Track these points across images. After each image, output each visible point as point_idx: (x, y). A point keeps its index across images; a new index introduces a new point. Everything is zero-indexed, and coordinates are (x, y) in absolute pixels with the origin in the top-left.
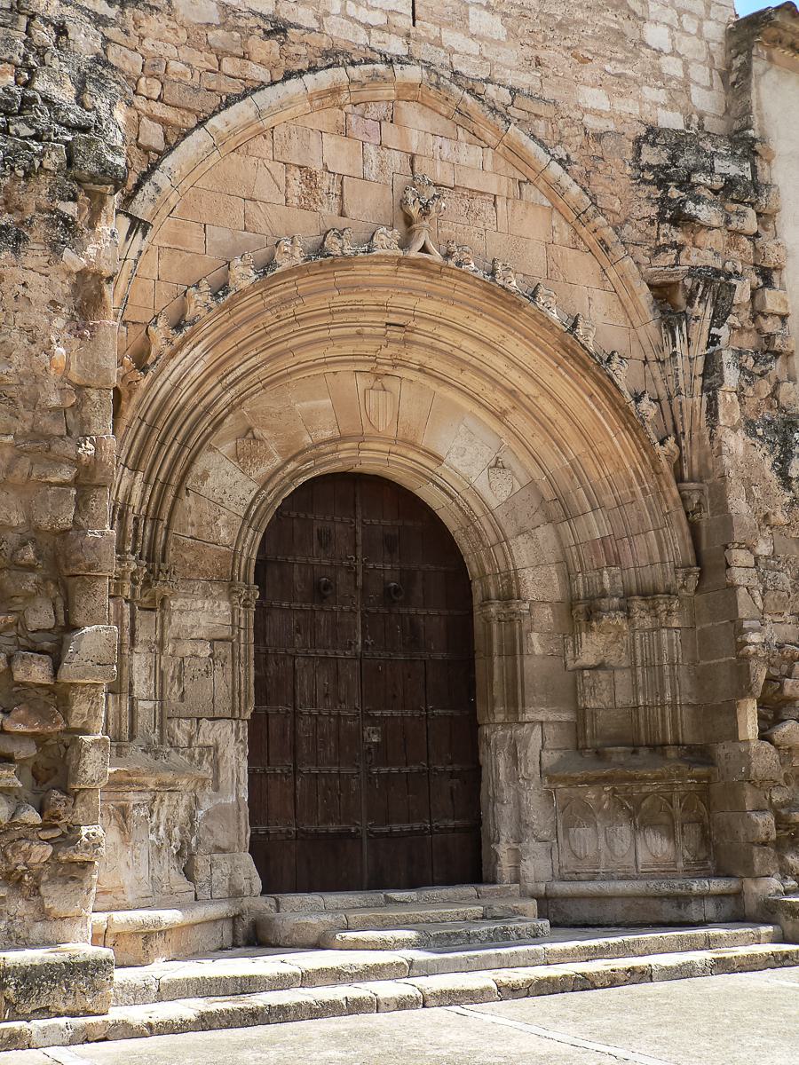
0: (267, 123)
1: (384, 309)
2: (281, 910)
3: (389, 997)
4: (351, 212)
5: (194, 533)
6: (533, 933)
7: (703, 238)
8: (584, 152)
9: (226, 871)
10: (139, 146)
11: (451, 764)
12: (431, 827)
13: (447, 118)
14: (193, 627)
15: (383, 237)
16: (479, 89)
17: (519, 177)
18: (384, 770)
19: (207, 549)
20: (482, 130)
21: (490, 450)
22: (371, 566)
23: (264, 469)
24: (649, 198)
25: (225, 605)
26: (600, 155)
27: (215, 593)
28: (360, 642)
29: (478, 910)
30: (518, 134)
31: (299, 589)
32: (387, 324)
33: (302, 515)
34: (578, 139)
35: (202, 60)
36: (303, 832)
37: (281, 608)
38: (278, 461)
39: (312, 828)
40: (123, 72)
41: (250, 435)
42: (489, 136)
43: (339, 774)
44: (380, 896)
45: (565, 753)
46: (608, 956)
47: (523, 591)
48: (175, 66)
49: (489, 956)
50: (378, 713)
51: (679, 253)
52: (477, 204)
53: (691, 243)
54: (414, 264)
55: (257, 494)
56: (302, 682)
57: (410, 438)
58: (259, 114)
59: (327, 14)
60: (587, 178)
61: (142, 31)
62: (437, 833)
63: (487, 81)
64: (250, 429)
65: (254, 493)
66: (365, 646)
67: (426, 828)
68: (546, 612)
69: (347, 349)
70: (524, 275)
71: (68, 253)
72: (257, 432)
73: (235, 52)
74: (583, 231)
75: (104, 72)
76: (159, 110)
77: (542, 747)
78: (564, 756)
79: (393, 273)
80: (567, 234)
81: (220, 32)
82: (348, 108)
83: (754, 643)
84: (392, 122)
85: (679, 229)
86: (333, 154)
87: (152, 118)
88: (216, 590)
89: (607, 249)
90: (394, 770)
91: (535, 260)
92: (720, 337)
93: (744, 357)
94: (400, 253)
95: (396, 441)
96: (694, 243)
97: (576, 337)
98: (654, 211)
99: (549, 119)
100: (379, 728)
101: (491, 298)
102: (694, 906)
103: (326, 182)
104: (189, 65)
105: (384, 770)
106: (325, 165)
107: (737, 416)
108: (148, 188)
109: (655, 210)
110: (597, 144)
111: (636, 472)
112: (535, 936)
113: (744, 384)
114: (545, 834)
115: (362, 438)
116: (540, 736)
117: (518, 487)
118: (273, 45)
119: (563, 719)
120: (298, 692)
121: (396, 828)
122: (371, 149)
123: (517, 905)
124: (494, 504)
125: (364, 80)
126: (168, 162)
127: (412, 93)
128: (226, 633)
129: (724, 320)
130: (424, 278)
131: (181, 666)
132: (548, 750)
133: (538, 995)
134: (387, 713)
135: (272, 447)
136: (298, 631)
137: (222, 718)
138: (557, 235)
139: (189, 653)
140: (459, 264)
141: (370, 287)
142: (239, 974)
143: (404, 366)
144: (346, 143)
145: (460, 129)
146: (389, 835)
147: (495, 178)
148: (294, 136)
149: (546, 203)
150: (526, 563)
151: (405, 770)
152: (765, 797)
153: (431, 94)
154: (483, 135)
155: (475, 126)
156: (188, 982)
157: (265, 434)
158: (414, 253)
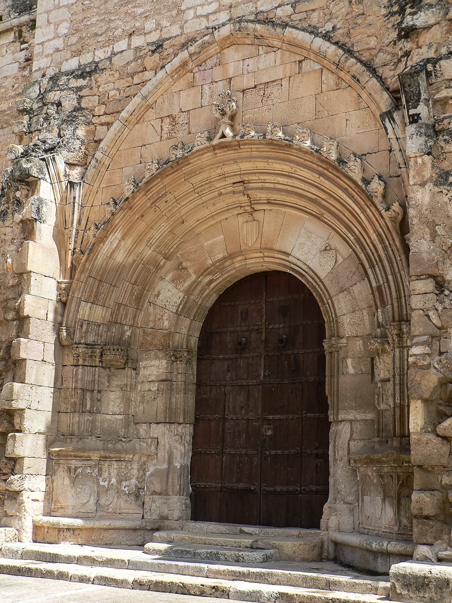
0: (151, 101)
1: (223, 177)
2: (184, 529)
3: (76, 574)
4: (193, 130)
5: (152, 326)
6: (236, 559)
7: (425, 38)
8: (349, 16)
9: (158, 505)
10: (96, 142)
11: (317, 449)
12: (301, 489)
13: (252, 45)
14: (149, 375)
15: (198, 139)
16: (271, 15)
17: (298, 58)
18: (273, 452)
19: (157, 333)
20: (271, 41)
21: (321, 240)
22: (271, 327)
23: (186, 284)
24: (393, 26)
25: (164, 362)
26: (361, 12)
27: (161, 356)
28: (262, 374)
29: (248, 541)
30: (291, 32)
31: (229, 347)
32: (234, 183)
33: (232, 304)
34: (343, 10)
35: (122, 84)
36: (224, 487)
37: (219, 359)
38: (194, 277)
39: (229, 485)
40: (88, 109)
41: (180, 267)
42: (276, 43)
43: (246, 455)
44: (237, 528)
45: (368, 442)
46: (248, 580)
47: (341, 331)
48: (112, 93)
49: (171, 565)
50: (271, 417)
51: (407, 58)
52: (268, 91)
53: (416, 46)
54: (222, 146)
55: (184, 298)
56: (229, 400)
57: (268, 246)
58: (145, 98)
59: (186, 22)
60: (348, 34)
61: (98, 84)
62: (304, 494)
63: (280, 6)
64: (181, 264)
65: (181, 299)
66: (264, 375)
67: (297, 490)
68: (358, 343)
69: (221, 205)
70: (298, 123)
71: (16, 215)
72: (184, 264)
73: (138, 71)
74: (342, 74)
75: (77, 114)
76: (104, 119)
77: (351, 438)
78: (367, 444)
79: (214, 156)
80: (332, 81)
81: (133, 64)
82: (196, 70)
83: (415, 355)
84: (219, 65)
85: (409, 40)
86: (186, 99)
87: (102, 124)
88: (160, 354)
89: (358, 81)
90: (279, 452)
91: (307, 110)
92: (420, 114)
93: (446, 121)
94: (207, 144)
95: (261, 250)
96: (418, 46)
97: (321, 154)
98: (394, 35)
99: (322, 8)
100: (272, 426)
101: (274, 148)
102: (380, 561)
103: (182, 119)
104: (118, 89)
105: (273, 452)
106: (181, 109)
107: (428, 173)
108: (93, 162)
109: (397, 32)
110: (358, 6)
111: (379, 235)
112: (237, 561)
113: (442, 144)
114: (350, 499)
115: (241, 253)
116: (349, 431)
117: (340, 260)
118: (157, 55)
119: (368, 418)
120: (226, 407)
121: (278, 488)
122: (206, 87)
123: (275, 542)
124: (322, 275)
125: (197, 50)
126: (102, 145)
127: (228, 42)
128: (164, 377)
129: (418, 100)
130: (233, 152)
131: (143, 397)
132: (354, 440)
133: (156, 591)
134: (278, 417)
135: (191, 271)
136: (229, 371)
137: (161, 423)
138: (324, 86)
139: (147, 389)
140: (242, 137)
141: (201, 170)
142: (52, 552)
143: (259, 203)
144: (193, 91)
145: (260, 48)
146: (275, 493)
147: (281, 68)
148: (166, 102)
149: (318, 67)
150: (345, 311)
151: (286, 452)
152: (438, 480)
153: (239, 36)
154: (273, 44)
155: (267, 41)
156: (33, 552)
157: (188, 265)
158: (216, 142)
